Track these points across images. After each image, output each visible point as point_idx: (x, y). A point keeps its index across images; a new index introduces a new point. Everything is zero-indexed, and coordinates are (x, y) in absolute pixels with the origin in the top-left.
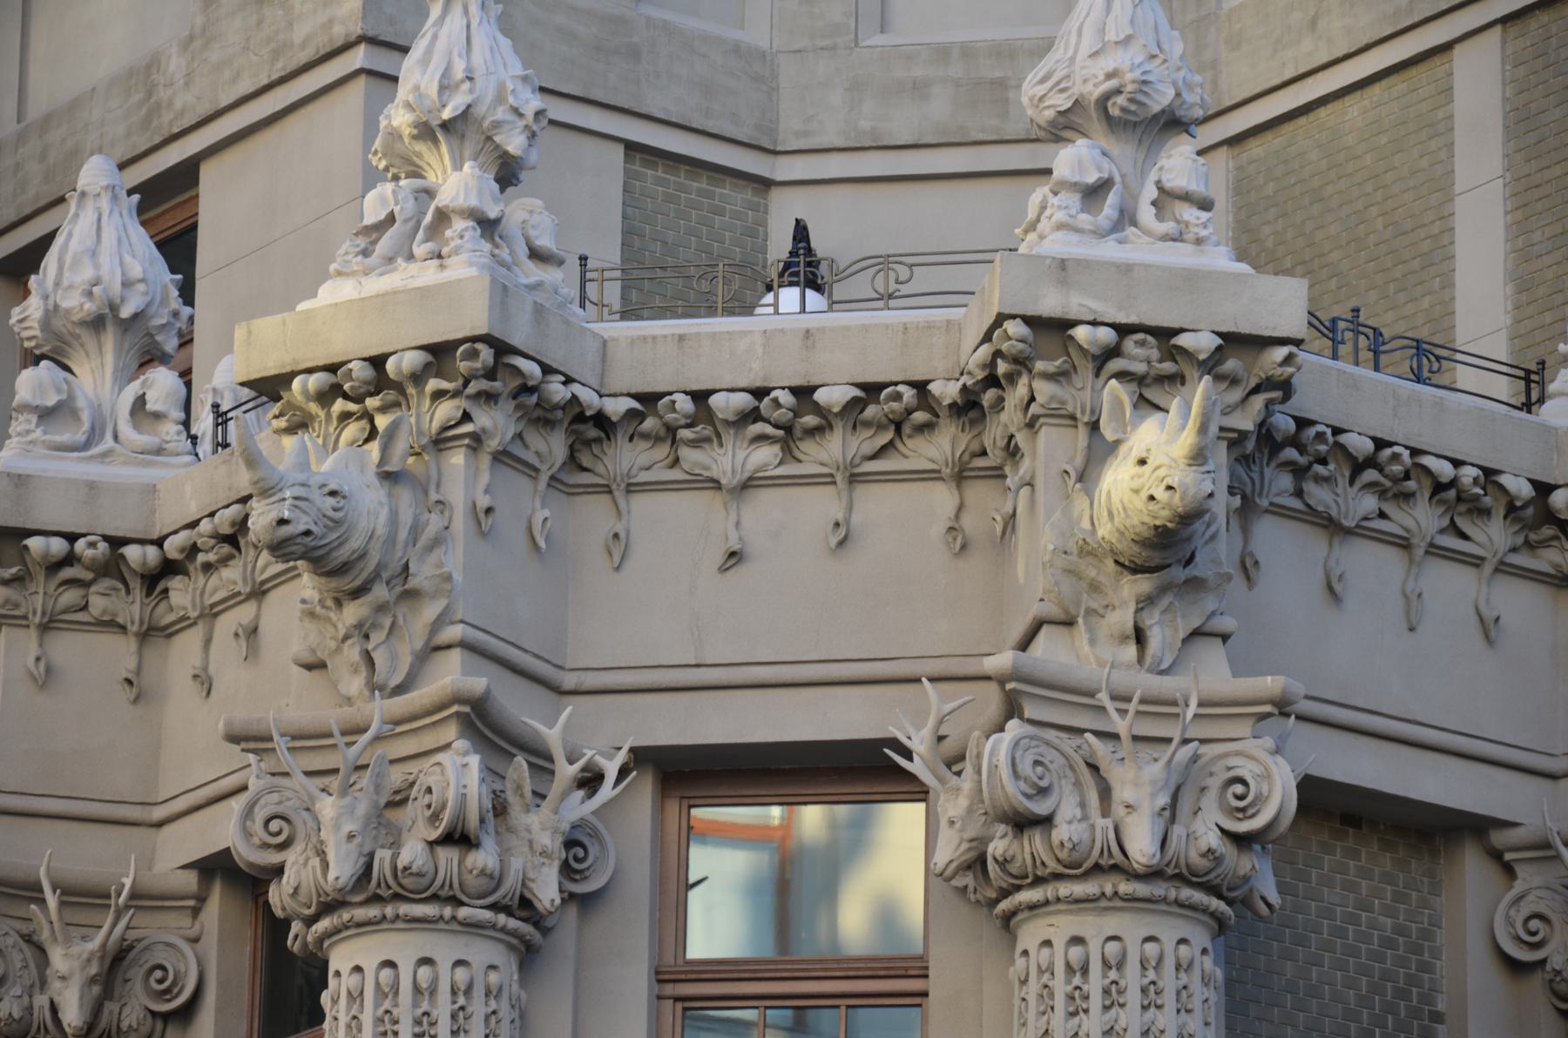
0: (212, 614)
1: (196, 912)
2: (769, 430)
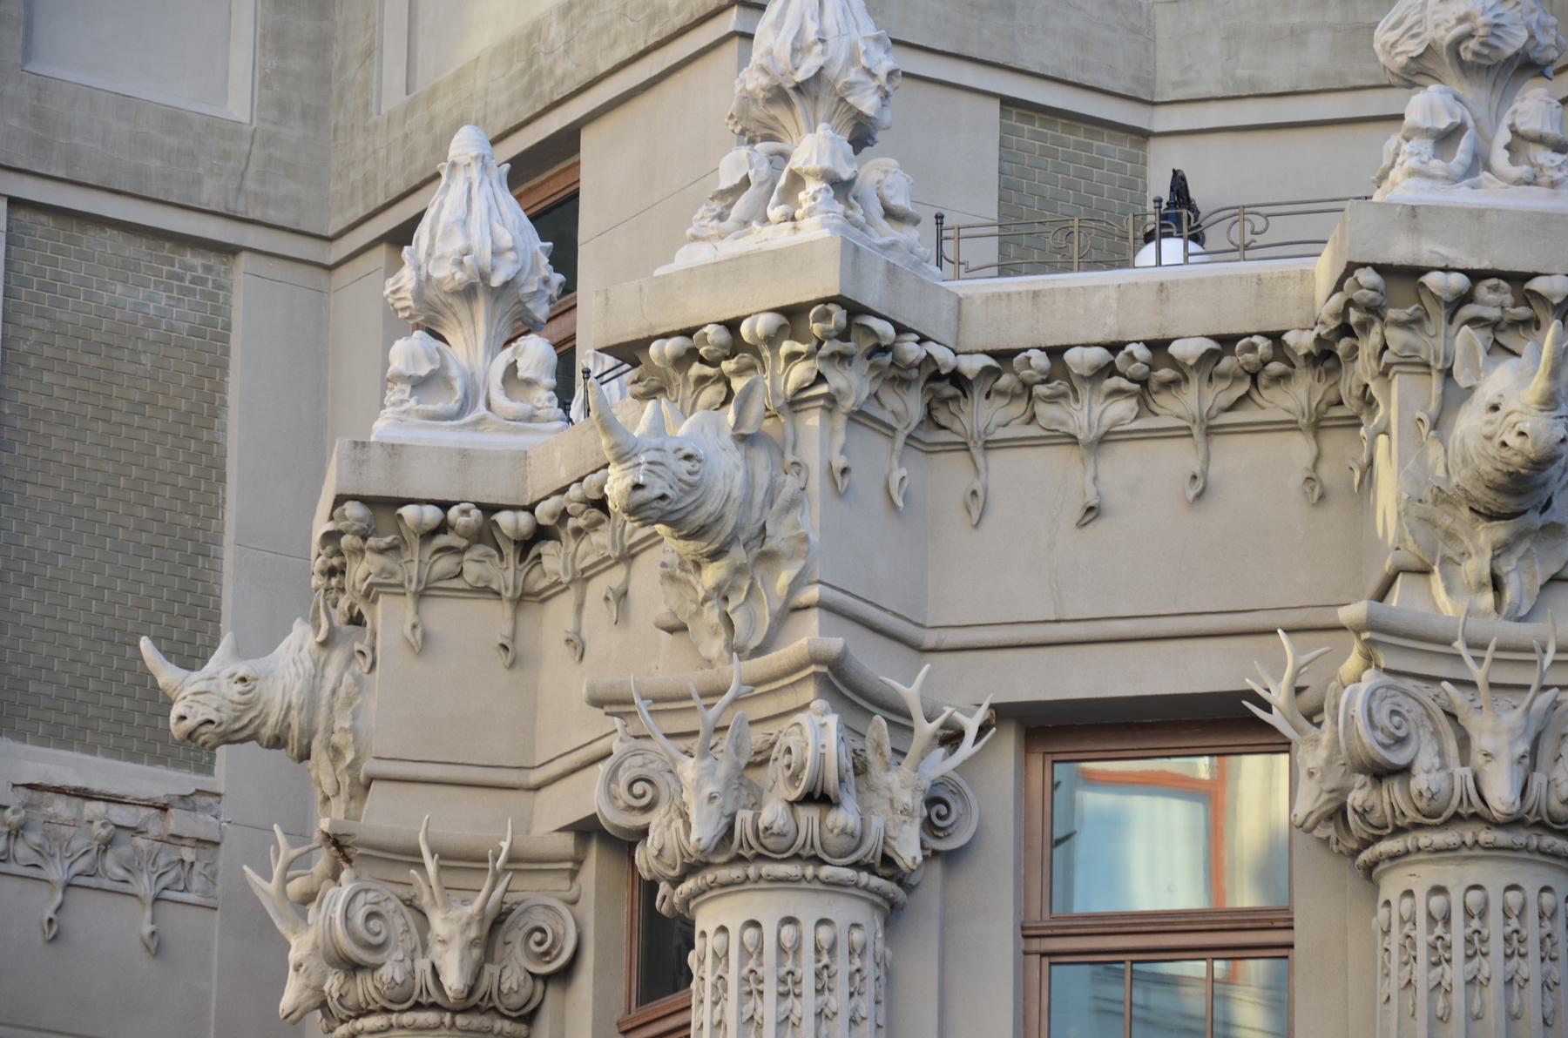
0: (583, 578)
1: (573, 874)
2: (1124, 384)
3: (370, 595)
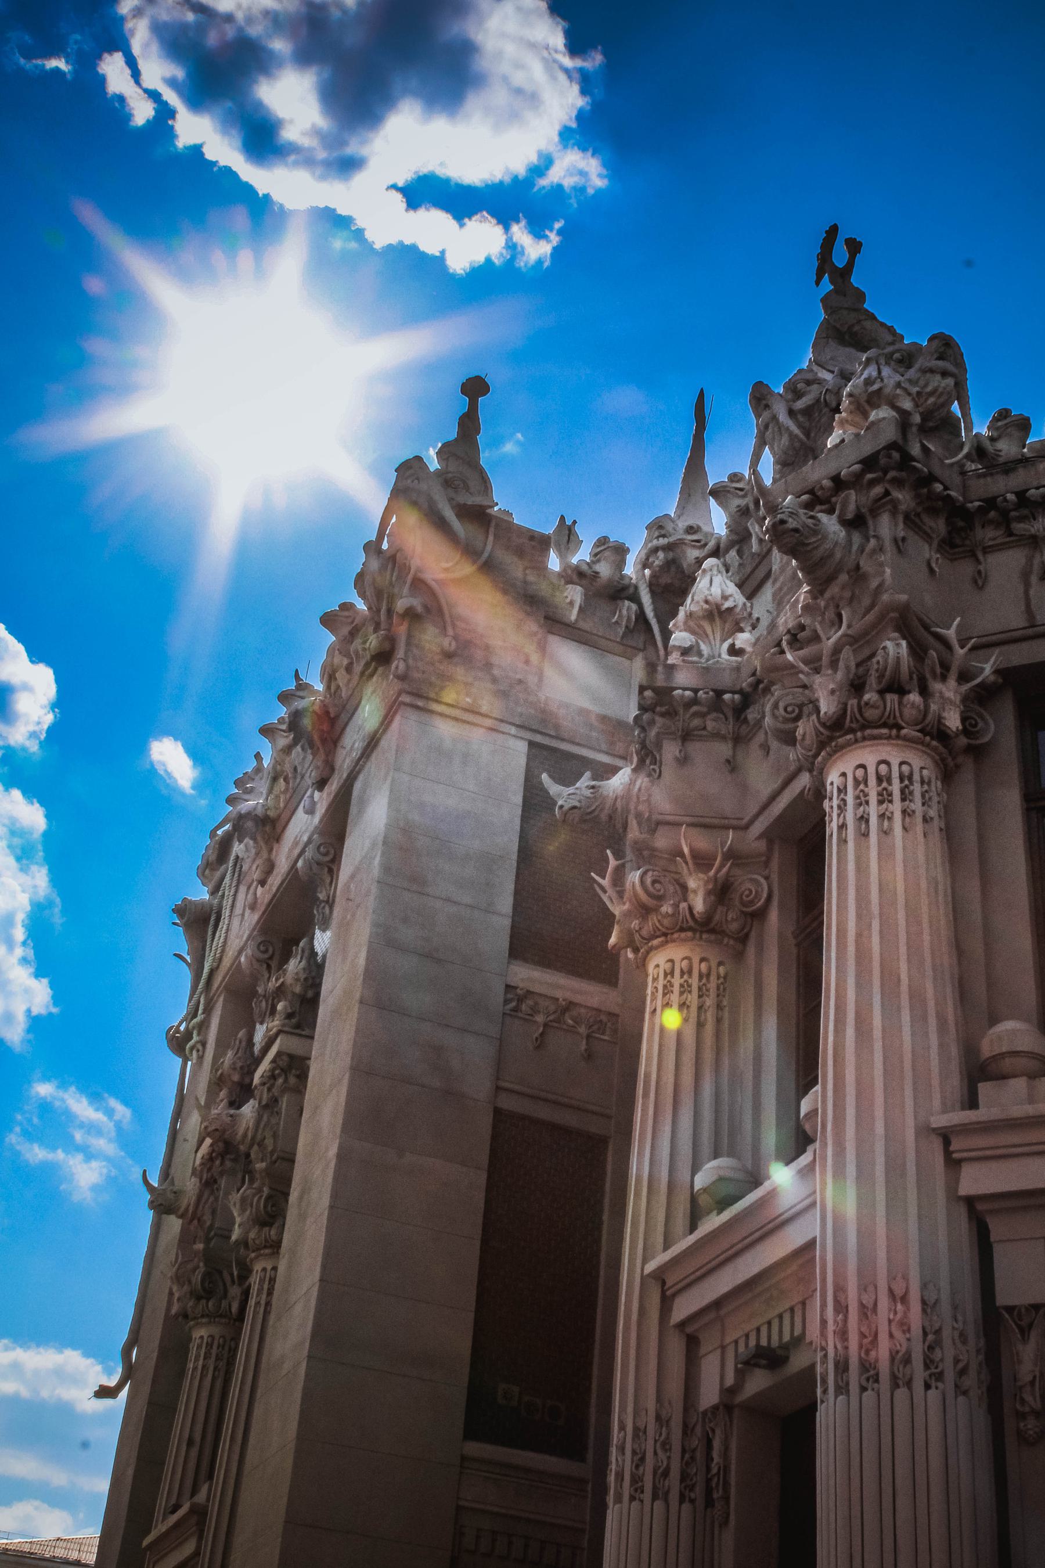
1: (767, 864)
3: (659, 745)
